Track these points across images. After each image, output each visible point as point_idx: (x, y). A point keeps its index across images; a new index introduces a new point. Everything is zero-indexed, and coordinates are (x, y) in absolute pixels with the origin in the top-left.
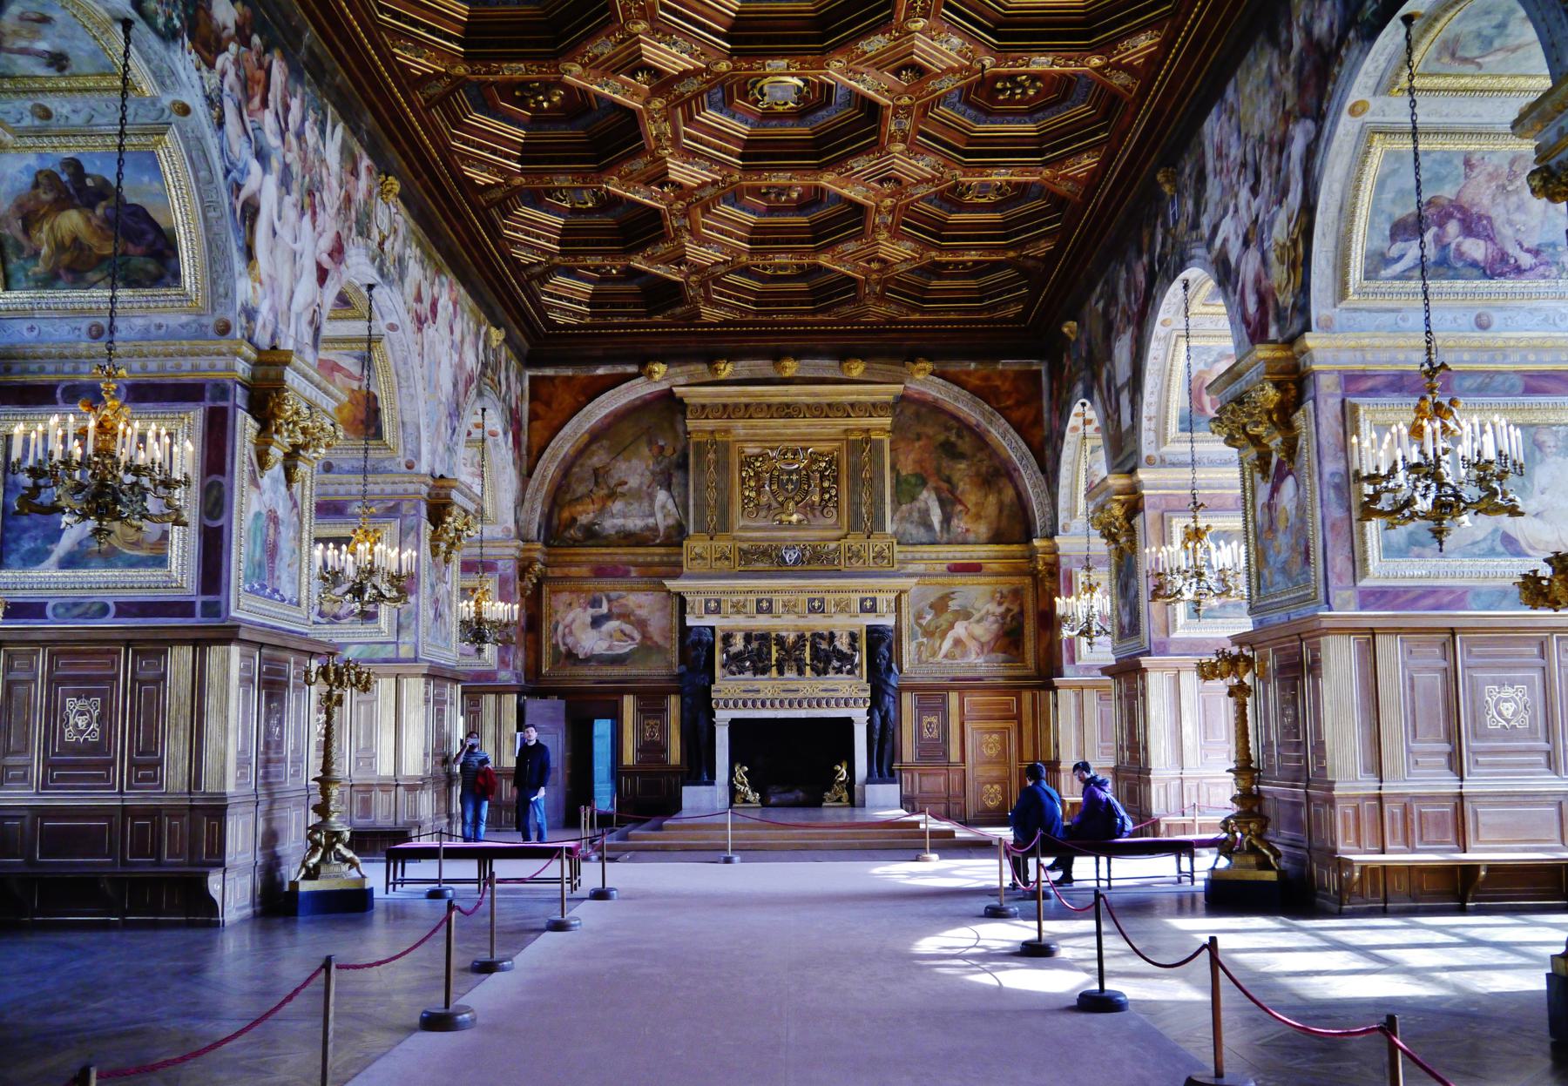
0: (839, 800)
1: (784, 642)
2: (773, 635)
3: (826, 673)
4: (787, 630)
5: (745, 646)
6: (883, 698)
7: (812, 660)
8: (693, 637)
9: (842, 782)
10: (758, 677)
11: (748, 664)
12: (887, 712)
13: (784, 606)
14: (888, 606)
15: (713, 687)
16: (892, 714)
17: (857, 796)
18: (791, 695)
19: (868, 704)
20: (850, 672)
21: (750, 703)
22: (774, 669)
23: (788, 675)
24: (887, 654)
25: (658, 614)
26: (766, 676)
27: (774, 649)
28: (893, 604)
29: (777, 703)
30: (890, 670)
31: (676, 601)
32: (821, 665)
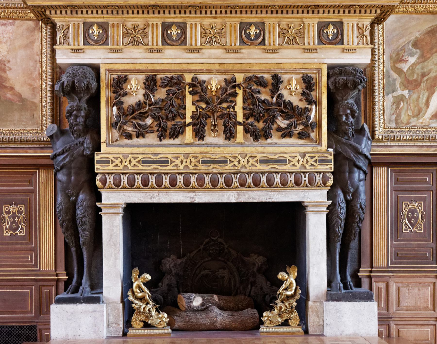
0: (285, 324)
1: (204, 90)
2: (188, 78)
3: (267, 136)
4: (209, 71)
5: (146, 96)
6: (351, 172)
7: (246, 117)
8: (64, 78)
9: (288, 298)
10: (166, 141)
11: (149, 121)
12: (356, 193)
13: (204, 34)
14: (361, 35)
15: (96, 158)
16: (363, 197)
17: (312, 318)
18: (217, 168)
19: (330, 182)
20: (301, 136)
21: (152, 180)
22: (189, 130)
23: (210, 139)
24: (356, 108)
25: (22, 53)
26: (177, 141)
27: (189, 99)
28: (367, 33)
29: (194, 179)
30: (360, 131)
31: (47, 31)
32: (261, 125)
